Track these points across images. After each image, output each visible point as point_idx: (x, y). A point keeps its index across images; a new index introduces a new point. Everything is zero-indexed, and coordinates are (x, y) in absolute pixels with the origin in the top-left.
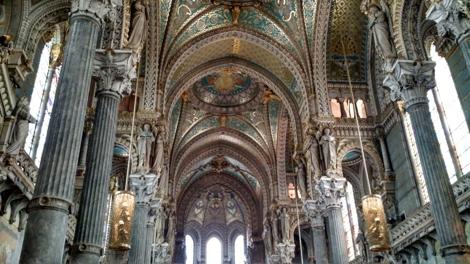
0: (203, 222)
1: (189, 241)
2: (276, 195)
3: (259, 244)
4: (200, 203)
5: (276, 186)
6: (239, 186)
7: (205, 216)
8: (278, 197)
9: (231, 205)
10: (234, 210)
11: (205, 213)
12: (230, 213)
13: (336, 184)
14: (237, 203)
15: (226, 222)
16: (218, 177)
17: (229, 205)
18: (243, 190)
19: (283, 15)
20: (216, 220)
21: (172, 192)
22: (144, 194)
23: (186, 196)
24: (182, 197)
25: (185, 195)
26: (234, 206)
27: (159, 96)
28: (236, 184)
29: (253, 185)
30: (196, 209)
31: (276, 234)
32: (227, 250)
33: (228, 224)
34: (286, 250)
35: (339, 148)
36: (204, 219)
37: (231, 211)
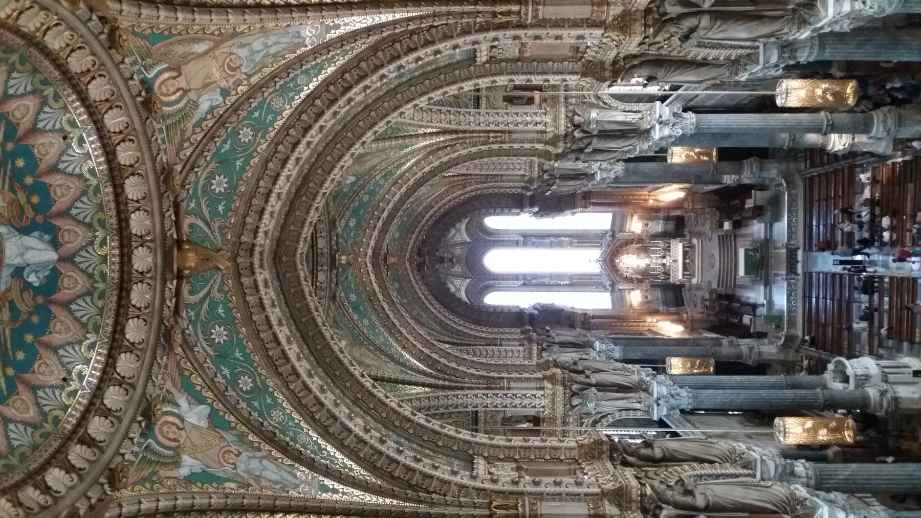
0: (466, 278)
1: (493, 299)
2: (518, 178)
5: (504, 178)
8: (524, 176)
12: (453, 237)
13: (664, 118)
15: (465, 242)
19: (355, 175)
21: (515, 339)
22: (678, 398)
27: (512, 384)
31: (579, 182)
32: (507, 241)
33: (468, 240)
34: (605, 170)
35: (601, 104)
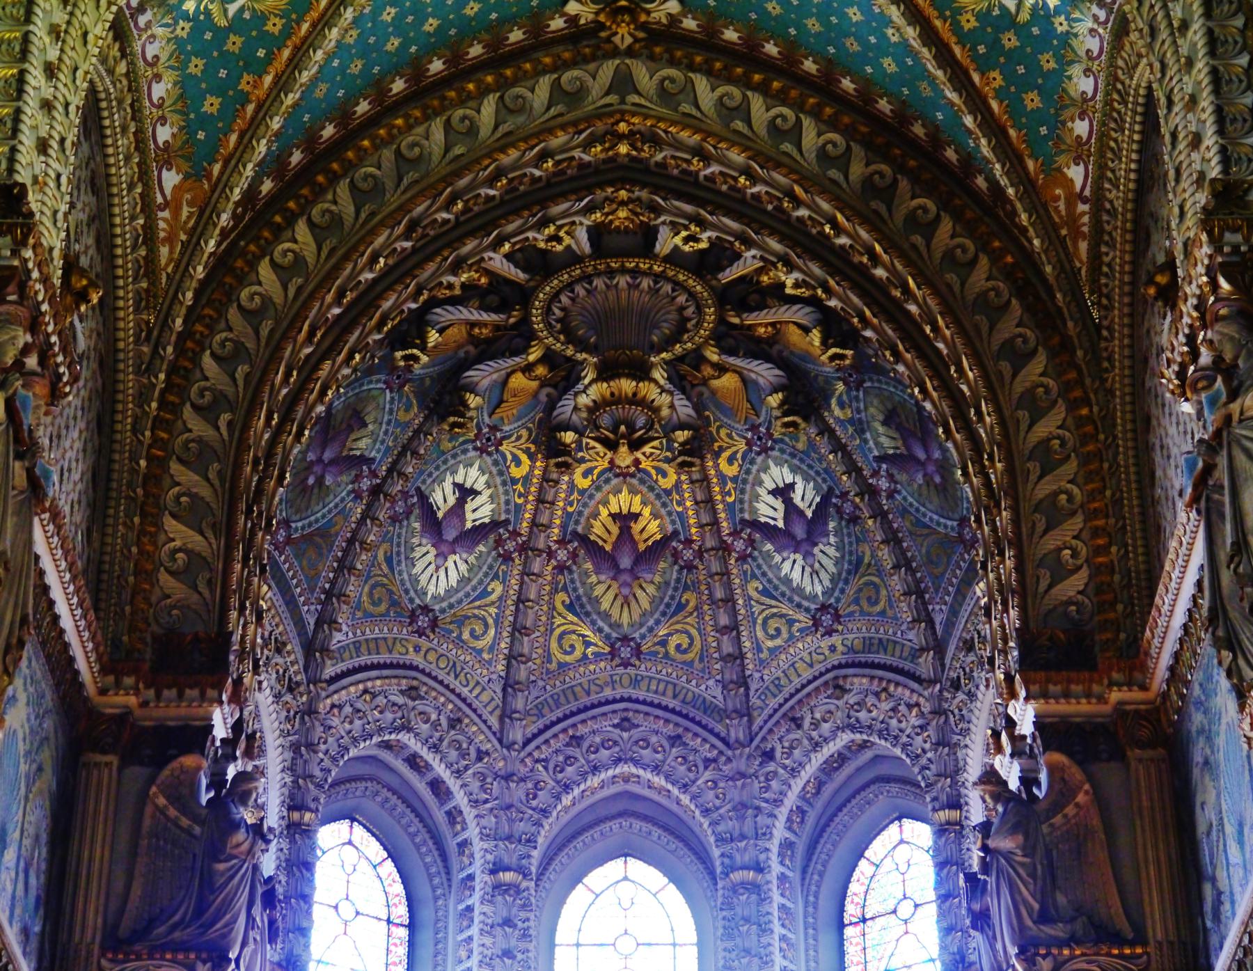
0: (509, 685)
3: (1119, 755)
4: (465, 493)
6: (857, 170)
7: (519, 630)
9: (791, 510)
10: (827, 552)
11: (521, 600)
14: (853, 469)
16: (622, 83)
17: (769, 510)
18: (911, 201)
20: (644, 669)
23: (265, 270)
24: (220, 263)
25: (253, 265)
26: (821, 510)
28: (822, 154)
29: (1016, 107)
30: (425, 552)
36: (513, 657)
37: (792, 568)
